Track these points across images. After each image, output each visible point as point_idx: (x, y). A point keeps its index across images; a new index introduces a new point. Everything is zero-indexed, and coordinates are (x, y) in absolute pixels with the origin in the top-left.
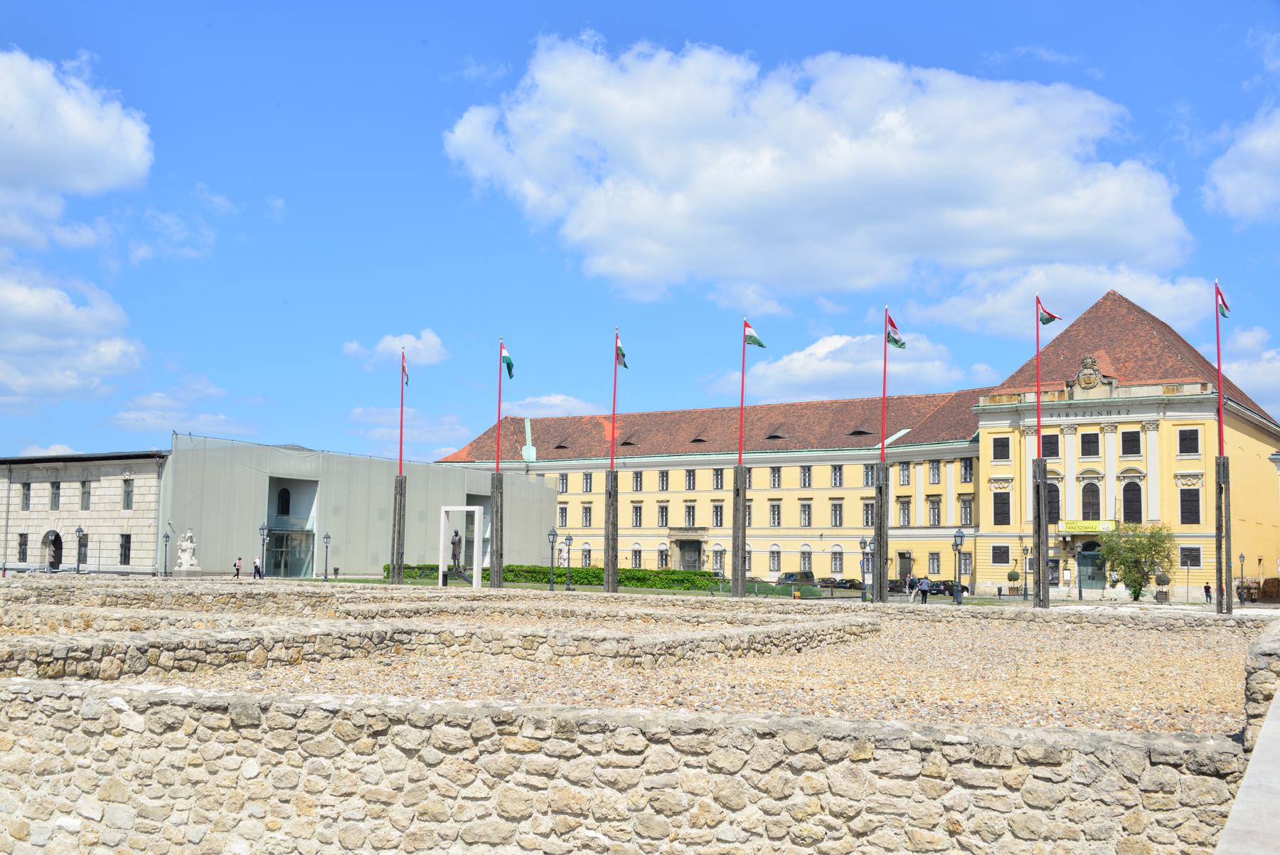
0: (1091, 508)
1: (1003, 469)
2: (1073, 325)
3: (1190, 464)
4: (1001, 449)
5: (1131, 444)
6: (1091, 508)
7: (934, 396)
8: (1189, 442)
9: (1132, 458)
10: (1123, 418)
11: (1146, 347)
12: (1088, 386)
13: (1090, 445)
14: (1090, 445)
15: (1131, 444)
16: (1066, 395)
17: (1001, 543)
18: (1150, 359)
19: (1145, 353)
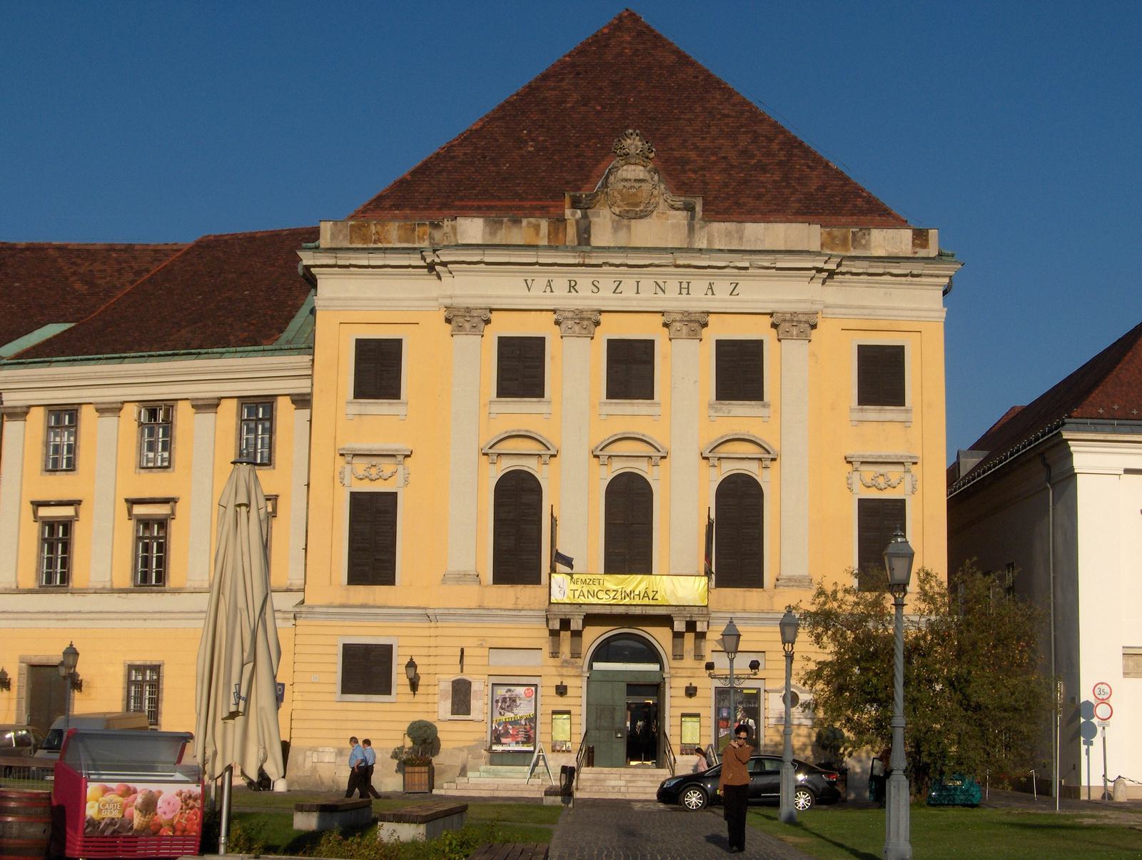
0: (629, 541)
1: (379, 424)
2: (545, 77)
3: (882, 431)
4: (378, 369)
5: (740, 372)
6: (629, 541)
7: (129, 248)
8: (881, 376)
9: (741, 409)
10: (722, 297)
11: (744, 141)
12: (634, 211)
13: (630, 370)
14: (630, 370)
15: (740, 372)
16: (571, 231)
17: (367, 634)
18: (763, 169)
19: (744, 153)
